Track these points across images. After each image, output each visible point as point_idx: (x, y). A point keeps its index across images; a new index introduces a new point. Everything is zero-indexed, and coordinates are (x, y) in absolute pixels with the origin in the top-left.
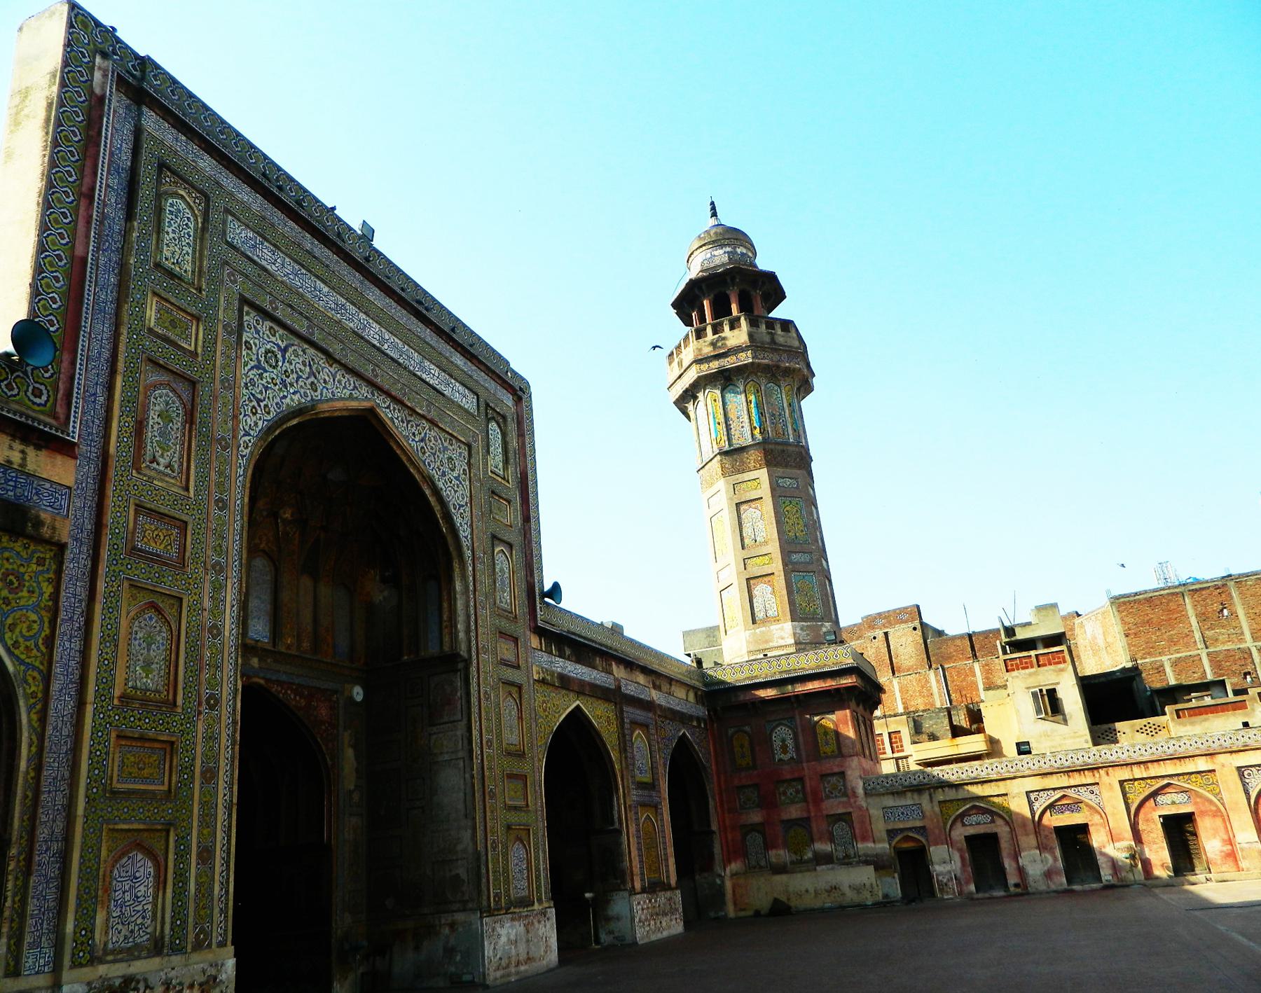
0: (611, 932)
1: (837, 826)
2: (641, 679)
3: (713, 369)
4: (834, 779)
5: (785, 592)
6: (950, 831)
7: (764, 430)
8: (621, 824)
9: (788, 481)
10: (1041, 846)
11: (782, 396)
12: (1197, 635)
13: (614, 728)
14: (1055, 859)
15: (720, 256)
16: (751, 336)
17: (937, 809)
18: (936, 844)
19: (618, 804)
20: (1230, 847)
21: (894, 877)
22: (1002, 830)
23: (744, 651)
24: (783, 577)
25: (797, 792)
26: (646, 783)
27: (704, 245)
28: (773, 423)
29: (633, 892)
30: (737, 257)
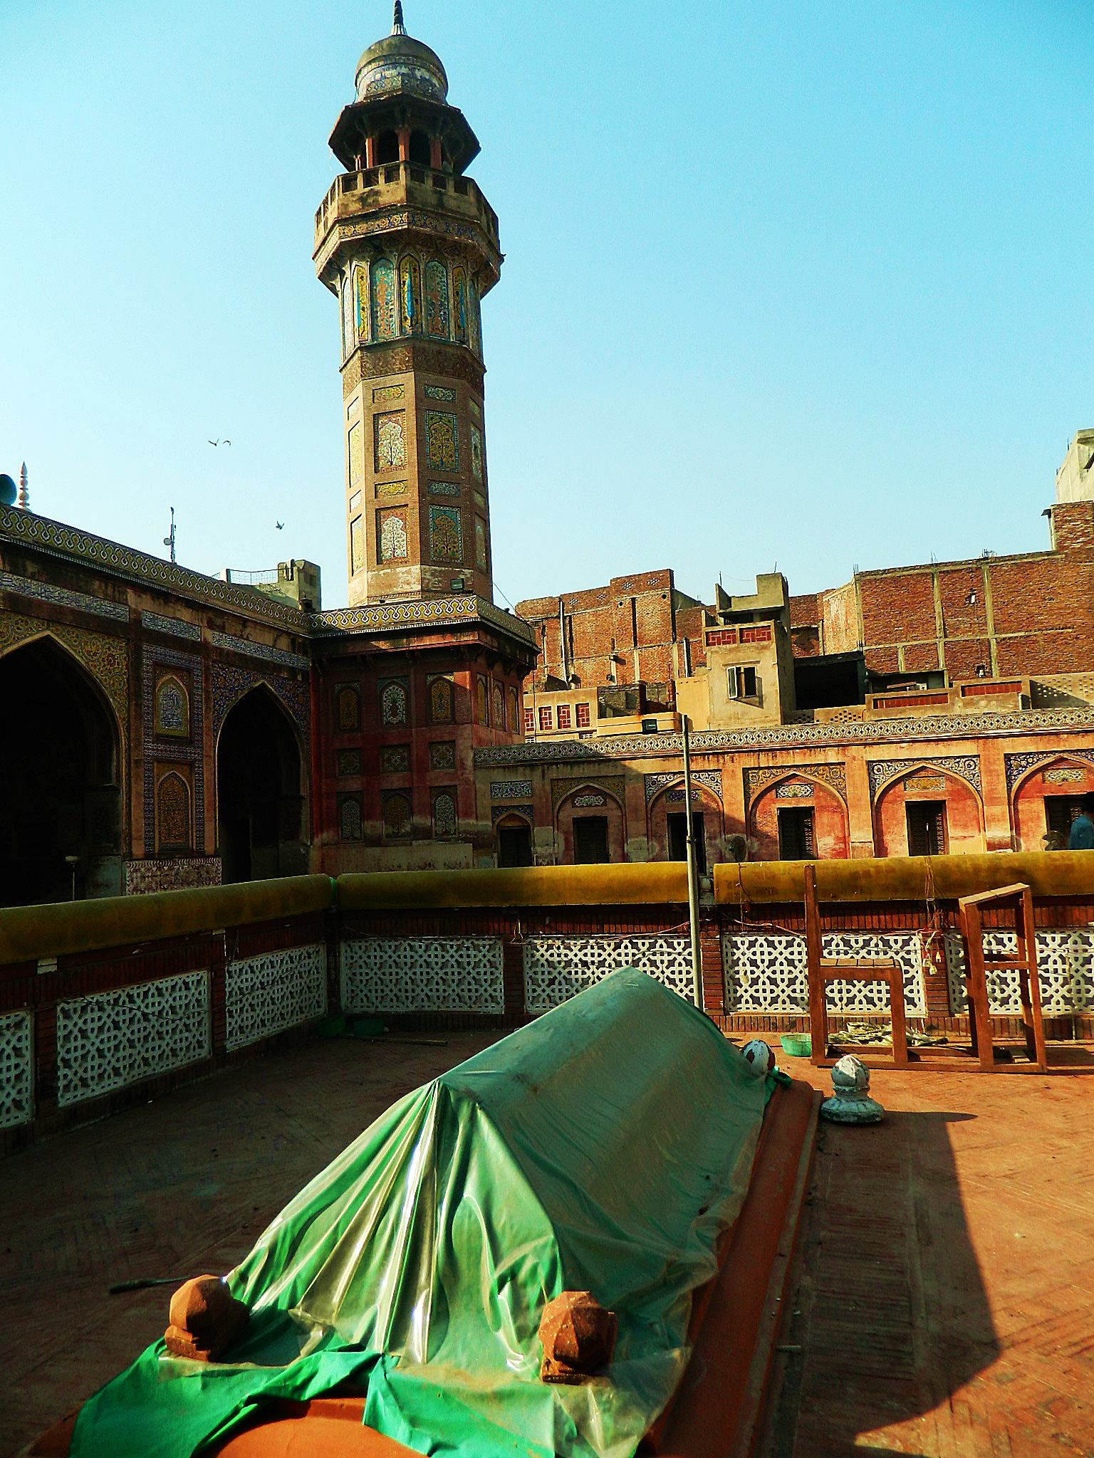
2: (186, 614)
4: (443, 748)
6: (558, 812)
9: (441, 392)
10: (650, 833)
11: (447, 279)
12: (939, 622)
14: (663, 848)
15: (391, 78)
16: (409, 191)
18: (541, 825)
20: (842, 845)
22: (612, 814)
23: (366, 595)
25: (403, 759)
27: (374, 60)
28: (430, 315)
29: (130, 857)
30: (414, 83)
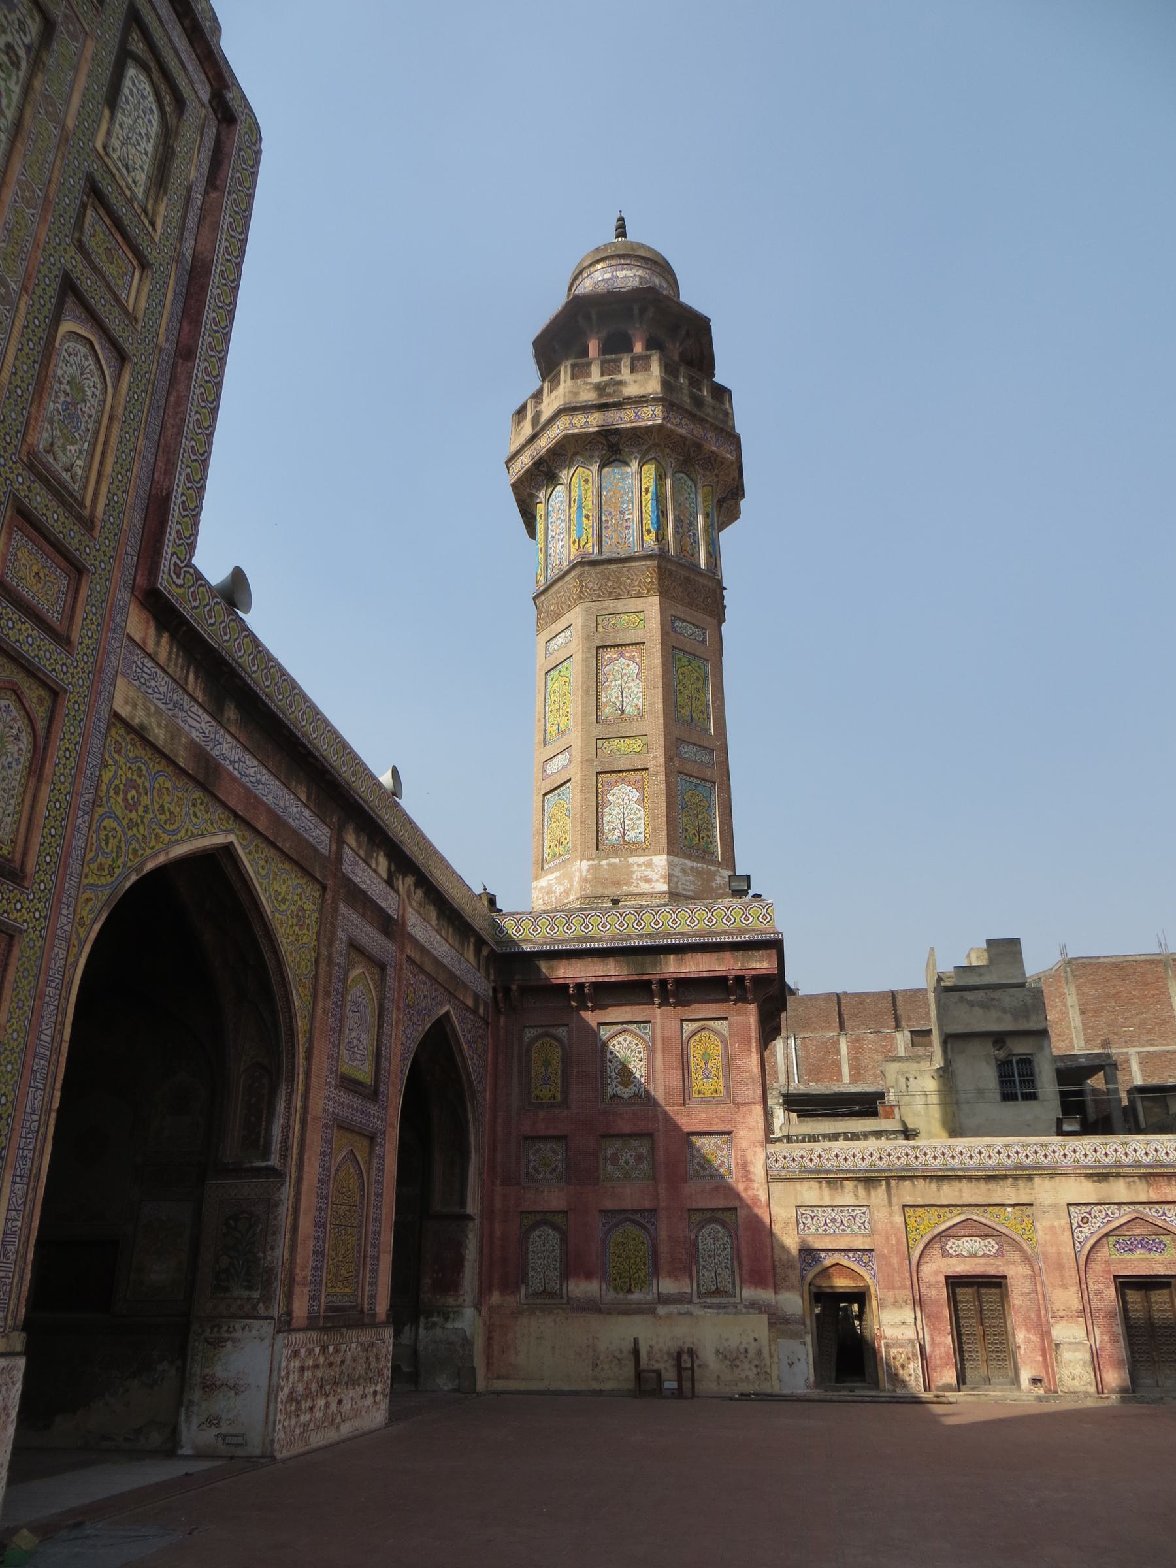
0: (213, 1421)
1: (706, 1231)
3: (592, 426)
5: (662, 802)
7: (663, 539)
8: (284, 1157)
9: (690, 629)
13: (309, 938)
15: (628, 277)
16: (665, 384)
17: (898, 1219)
19: (288, 1108)
21: (804, 1343)
22: (1015, 1272)
24: (663, 778)
25: (639, 1159)
26: (360, 1083)
29: (285, 1325)
